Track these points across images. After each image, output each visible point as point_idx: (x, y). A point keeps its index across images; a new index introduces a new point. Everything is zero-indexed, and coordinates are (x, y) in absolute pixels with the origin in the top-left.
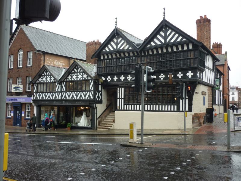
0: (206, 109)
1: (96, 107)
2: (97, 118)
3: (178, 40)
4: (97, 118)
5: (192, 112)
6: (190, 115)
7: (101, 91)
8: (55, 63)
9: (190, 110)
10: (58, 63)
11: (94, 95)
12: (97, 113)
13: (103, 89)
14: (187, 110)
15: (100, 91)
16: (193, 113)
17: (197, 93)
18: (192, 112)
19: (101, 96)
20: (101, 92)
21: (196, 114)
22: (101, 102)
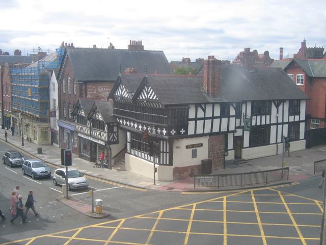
0: (200, 160)
1: (111, 149)
2: (112, 157)
3: (154, 98)
4: (112, 157)
5: (172, 165)
6: (170, 169)
7: (118, 132)
8: (98, 90)
9: (171, 164)
10: (102, 88)
11: (109, 137)
12: (111, 154)
13: (119, 130)
14: (168, 163)
15: (115, 133)
16: (173, 167)
17: (177, 147)
18: (172, 165)
19: (117, 136)
20: (116, 133)
21: (176, 168)
22: (117, 142)
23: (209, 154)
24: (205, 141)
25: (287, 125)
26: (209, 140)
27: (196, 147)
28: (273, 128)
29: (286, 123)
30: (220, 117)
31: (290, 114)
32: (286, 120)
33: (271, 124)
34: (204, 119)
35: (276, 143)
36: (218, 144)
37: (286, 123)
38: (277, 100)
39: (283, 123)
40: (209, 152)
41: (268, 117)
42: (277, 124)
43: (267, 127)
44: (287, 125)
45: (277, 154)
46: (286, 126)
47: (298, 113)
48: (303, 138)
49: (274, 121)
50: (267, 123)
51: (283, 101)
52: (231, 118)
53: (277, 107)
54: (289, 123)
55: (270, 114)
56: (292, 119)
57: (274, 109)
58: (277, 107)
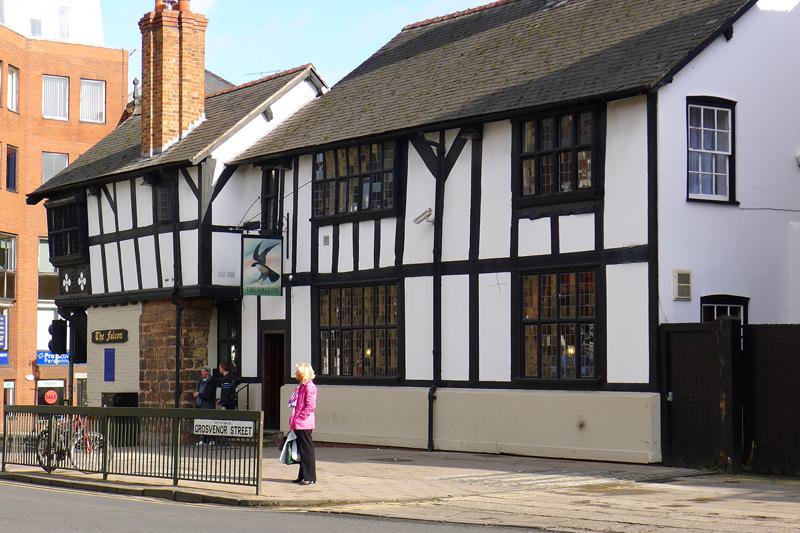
23: (141, 378)
24: (128, 318)
25: (505, 278)
26: (142, 320)
27: (111, 341)
28: (418, 290)
29: (494, 265)
30: (154, 230)
31: (524, 206)
32: (495, 246)
33: (402, 271)
34: (118, 237)
35: (437, 382)
36: (164, 339)
37: (494, 265)
38: (440, 127)
39: (474, 267)
40: (143, 365)
41: (389, 227)
42: (438, 269)
43: (390, 281)
44: (505, 278)
45: (431, 447)
46: (497, 289)
47: (592, 201)
48: (643, 376)
49: (418, 251)
50: (383, 264)
51: (472, 127)
52: (183, 234)
53: (441, 169)
54: (515, 265)
55: (399, 212)
56: (535, 239)
57: (419, 181)
58: (441, 169)
